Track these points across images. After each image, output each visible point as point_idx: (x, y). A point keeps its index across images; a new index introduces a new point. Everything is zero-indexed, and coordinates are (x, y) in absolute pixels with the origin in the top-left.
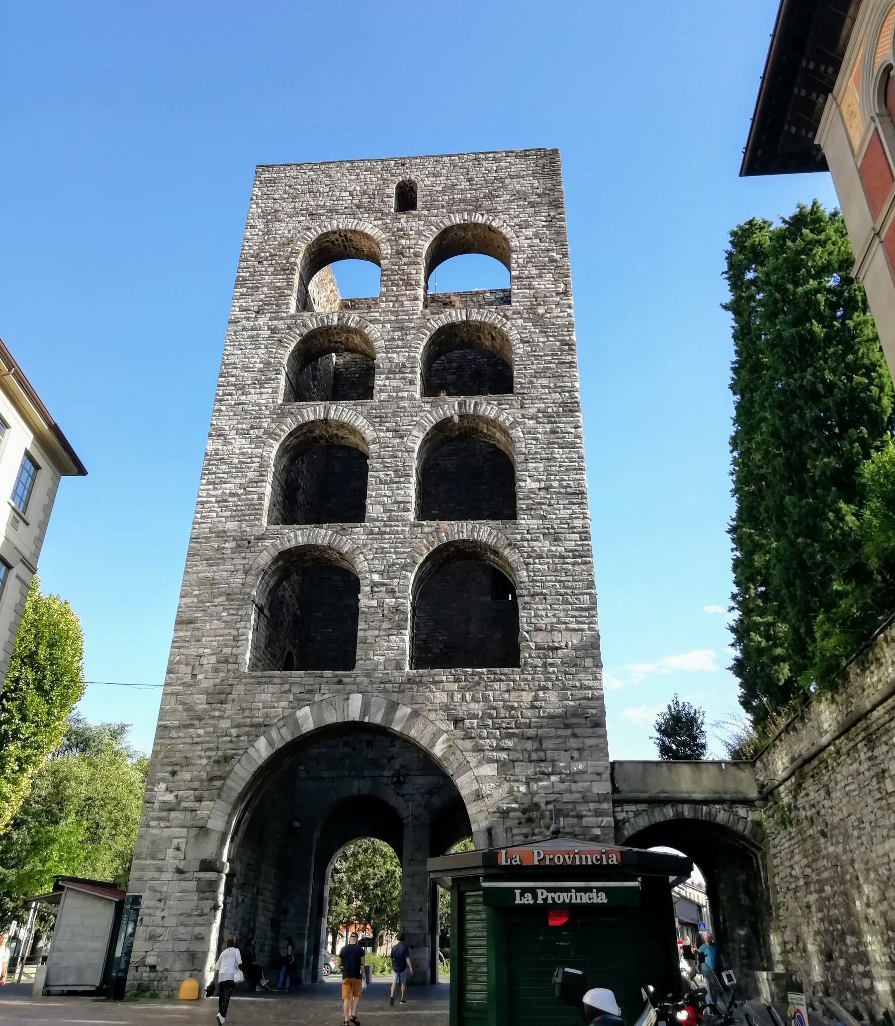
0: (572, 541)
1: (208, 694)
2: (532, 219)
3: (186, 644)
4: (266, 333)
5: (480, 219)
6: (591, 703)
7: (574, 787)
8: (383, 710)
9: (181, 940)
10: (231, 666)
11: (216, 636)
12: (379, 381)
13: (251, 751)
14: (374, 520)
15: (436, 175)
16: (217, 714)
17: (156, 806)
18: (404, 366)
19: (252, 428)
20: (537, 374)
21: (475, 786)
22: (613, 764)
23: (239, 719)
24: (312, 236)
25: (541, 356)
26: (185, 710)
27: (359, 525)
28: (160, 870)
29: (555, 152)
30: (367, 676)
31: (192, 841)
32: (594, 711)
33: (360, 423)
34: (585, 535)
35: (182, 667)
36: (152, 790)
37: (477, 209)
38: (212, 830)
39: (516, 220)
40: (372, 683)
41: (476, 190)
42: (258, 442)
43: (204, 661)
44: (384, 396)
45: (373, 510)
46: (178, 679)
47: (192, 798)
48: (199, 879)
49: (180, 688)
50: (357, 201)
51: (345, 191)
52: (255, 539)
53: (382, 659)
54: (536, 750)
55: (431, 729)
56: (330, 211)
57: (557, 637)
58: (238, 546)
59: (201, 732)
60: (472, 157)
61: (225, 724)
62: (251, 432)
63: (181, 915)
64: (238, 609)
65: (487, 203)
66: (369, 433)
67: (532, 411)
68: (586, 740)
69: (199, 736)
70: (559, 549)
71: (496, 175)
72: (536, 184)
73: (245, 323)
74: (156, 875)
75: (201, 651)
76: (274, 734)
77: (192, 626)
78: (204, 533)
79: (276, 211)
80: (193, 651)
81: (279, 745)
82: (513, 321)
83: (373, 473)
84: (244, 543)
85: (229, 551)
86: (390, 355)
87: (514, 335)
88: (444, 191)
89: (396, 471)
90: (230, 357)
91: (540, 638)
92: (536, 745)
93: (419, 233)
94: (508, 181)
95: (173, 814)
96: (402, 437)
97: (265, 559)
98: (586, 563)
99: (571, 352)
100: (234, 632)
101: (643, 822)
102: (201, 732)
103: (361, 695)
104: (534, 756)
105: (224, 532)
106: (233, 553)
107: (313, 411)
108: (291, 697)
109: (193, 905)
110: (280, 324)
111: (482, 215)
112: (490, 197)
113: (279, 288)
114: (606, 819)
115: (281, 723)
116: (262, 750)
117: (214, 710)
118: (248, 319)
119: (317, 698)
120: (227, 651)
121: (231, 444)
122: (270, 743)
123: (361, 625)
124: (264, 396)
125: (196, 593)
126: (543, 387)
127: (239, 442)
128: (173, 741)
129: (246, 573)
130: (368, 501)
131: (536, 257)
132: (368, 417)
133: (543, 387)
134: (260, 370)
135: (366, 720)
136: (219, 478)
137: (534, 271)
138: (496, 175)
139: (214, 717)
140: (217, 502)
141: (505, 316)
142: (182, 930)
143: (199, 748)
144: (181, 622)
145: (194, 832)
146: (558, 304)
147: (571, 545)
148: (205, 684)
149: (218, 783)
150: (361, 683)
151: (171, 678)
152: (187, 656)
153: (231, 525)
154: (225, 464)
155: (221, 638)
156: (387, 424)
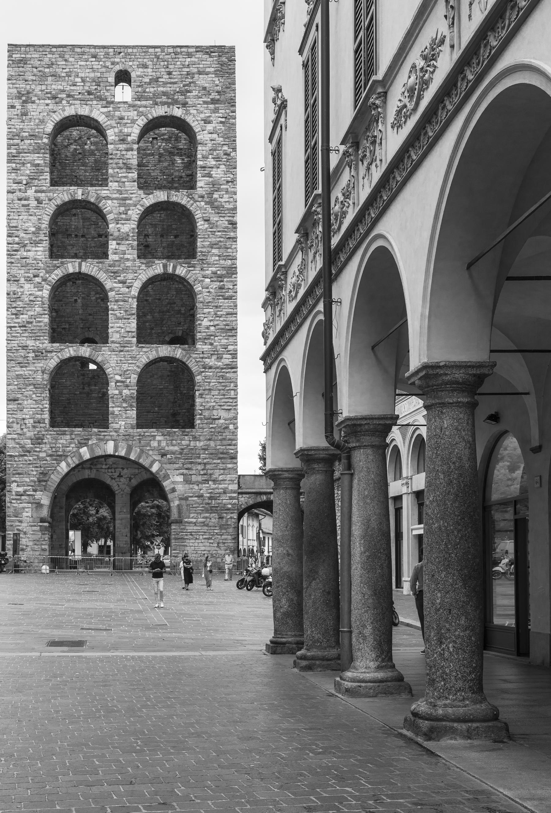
0: (227, 359)
1: (31, 439)
2: (213, 115)
3: (15, 412)
4: (33, 203)
5: (178, 112)
6: (230, 447)
7: (221, 486)
8: (125, 449)
9: (36, 551)
10: (42, 425)
11: (31, 408)
12: (112, 245)
13: (58, 468)
14: (113, 342)
15: (145, 66)
16: (38, 449)
17: (14, 493)
18: (128, 235)
19: (35, 276)
20: (212, 246)
21: (172, 486)
22: (240, 476)
23: (50, 452)
24: (57, 117)
25: (215, 232)
26: (20, 447)
27: (105, 345)
28: (21, 522)
29: (232, 49)
30: (116, 432)
31: (34, 509)
32: (232, 451)
33: (102, 276)
34: (234, 355)
35: (15, 425)
36: (10, 486)
37: (175, 102)
38: (44, 505)
39: (203, 116)
40: (118, 435)
41: (175, 83)
42: (39, 287)
43: (27, 421)
44: (116, 257)
45: (114, 335)
46: (14, 431)
47: (31, 490)
48: (41, 526)
49: (16, 436)
50: (87, 88)
51: (77, 76)
52: (46, 352)
53: (124, 423)
54: (203, 470)
55: (151, 459)
56: (69, 96)
57: (215, 413)
58: (36, 356)
59: (31, 458)
60: (171, 50)
61: (42, 455)
62: (33, 279)
63: (34, 541)
64: (41, 393)
65: (181, 98)
66: (108, 285)
67: (208, 272)
68: (228, 465)
69: (30, 460)
70: (220, 363)
71: (188, 70)
72: (217, 82)
73: (18, 194)
74: (19, 524)
75: (24, 416)
76: (69, 460)
77: (17, 402)
78: (14, 347)
79: (28, 93)
80: (19, 416)
81: (73, 465)
82: (198, 203)
83: (112, 312)
84: (39, 354)
85: (31, 359)
86: (118, 226)
87: (198, 215)
88: (149, 83)
89: (126, 311)
90: (12, 221)
91: (206, 413)
92: (203, 467)
93: (133, 121)
94: (196, 76)
95: (23, 497)
96: (128, 288)
97: (53, 363)
98: (234, 372)
99: (234, 230)
100: (41, 406)
101: (251, 502)
102: (31, 458)
103: (113, 442)
104: (202, 472)
105: (27, 346)
106: (34, 360)
107: (72, 266)
108: (76, 442)
109: (39, 536)
110: (42, 196)
111: (179, 108)
112: (184, 93)
113: (38, 165)
114: (234, 501)
115: (73, 455)
116: (64, 467)
117: (36, 447)
118: (20, 190)
119: (90, 442)
120: (39, 416)
121: (22, 287)
122: (68, 464)
123: (111, 405)
124: (39, 253)
125: (16, 383)
126: (216, 255)
127: (27, 286)
128: (17, 463)
129: (43, 372)
130: (110, 330)
131: (215, 150)
132: (107, 271)
133: (216, 255)
134: (33, 233)
135: (117, 454)
136: (18, 311)
137: (213, 163)
138: (188, 70)
139: (36, 451)
140: (20, 327)
141: (192, 198)
142: (36, 547)
143: (31, 466)
144: (10, 400)
145: (34, 505)
146: (227, 192)
147: (227, 361)
148: (29, 434)
149: (44, 483)
150: (113, 436)
151: (10, 431)
152: (16, 418)
153: (30, 343)
154: (20, 301)
155: (34, 410)
156: (118, 278)
